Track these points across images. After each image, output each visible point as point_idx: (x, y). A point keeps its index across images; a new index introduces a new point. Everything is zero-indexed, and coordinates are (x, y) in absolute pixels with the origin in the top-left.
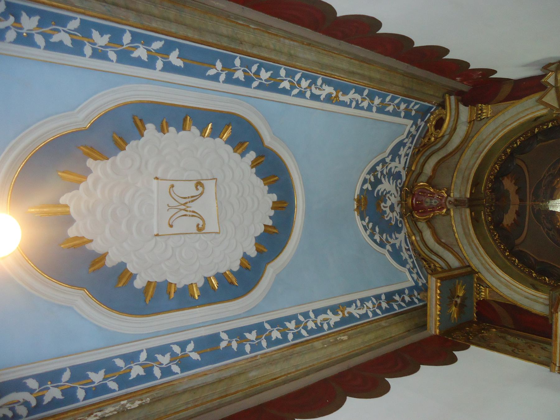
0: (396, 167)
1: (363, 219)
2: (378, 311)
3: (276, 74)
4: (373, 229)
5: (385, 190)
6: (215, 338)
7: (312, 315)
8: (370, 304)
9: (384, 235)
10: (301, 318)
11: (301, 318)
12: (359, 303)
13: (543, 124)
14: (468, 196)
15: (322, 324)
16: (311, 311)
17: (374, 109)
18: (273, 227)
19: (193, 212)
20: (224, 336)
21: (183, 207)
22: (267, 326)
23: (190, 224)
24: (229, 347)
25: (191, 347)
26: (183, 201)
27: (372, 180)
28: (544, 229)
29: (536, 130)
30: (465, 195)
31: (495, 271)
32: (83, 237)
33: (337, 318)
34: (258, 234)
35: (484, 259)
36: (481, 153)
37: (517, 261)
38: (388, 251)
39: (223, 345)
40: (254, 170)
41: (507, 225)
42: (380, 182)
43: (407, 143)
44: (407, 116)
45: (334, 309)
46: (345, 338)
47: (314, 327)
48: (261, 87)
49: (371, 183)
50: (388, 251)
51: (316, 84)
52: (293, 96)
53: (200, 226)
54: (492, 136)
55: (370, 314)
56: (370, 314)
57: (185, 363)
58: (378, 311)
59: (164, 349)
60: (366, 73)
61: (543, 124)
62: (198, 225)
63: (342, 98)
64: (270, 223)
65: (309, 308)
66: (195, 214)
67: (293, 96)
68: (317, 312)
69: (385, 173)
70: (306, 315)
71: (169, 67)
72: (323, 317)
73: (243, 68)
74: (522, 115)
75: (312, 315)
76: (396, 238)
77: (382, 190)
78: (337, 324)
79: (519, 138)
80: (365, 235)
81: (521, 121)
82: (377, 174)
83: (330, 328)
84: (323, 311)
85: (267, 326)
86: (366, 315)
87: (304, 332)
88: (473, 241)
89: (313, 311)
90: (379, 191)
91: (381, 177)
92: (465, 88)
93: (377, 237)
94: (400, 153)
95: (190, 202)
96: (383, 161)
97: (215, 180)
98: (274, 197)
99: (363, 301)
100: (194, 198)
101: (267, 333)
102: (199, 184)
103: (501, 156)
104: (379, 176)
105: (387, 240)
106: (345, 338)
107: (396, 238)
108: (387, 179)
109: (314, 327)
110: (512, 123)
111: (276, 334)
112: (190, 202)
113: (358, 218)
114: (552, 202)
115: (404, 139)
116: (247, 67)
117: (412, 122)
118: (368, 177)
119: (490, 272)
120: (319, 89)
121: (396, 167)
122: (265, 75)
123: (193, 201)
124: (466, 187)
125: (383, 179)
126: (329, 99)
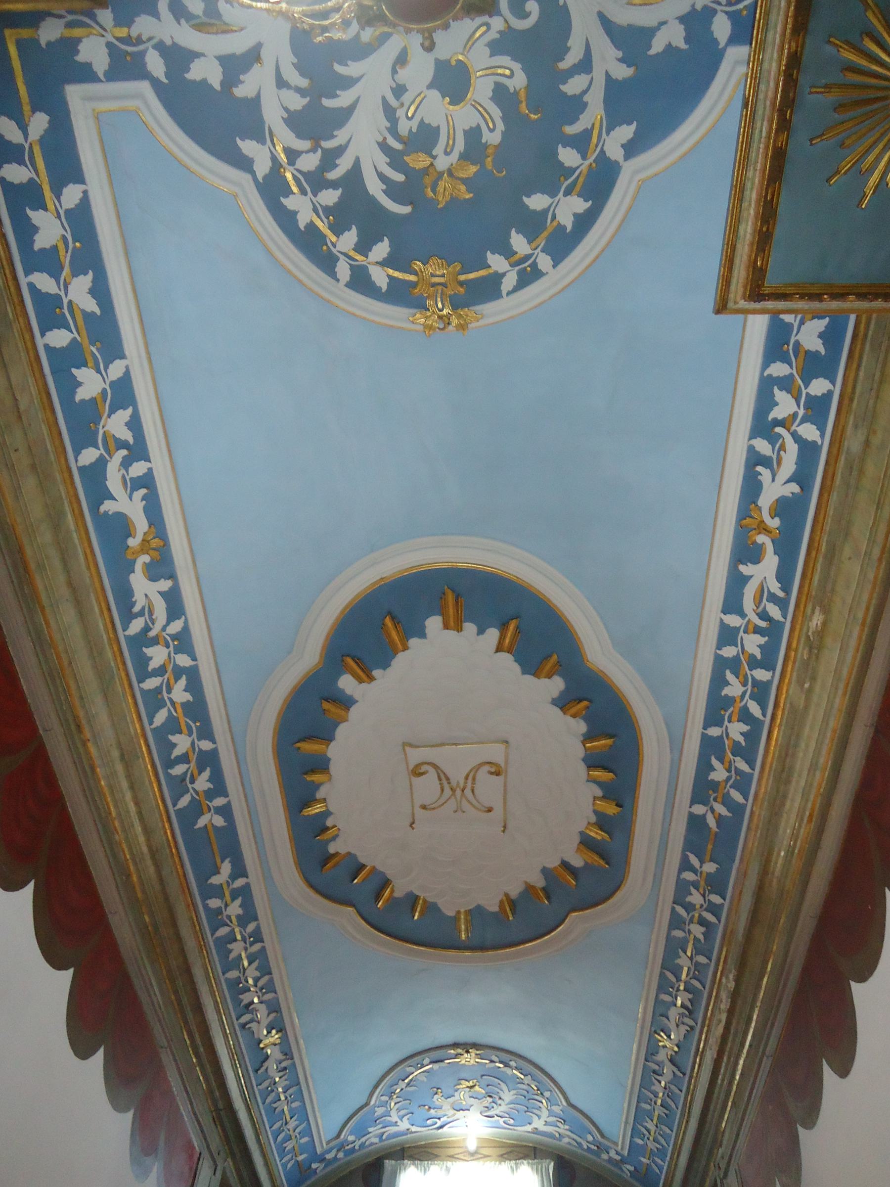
0: (281, 83)
1: (489, 289)
2: (819, 387)
3: (172, 725)
4: (533, 224)
5: (384, 146)
6: (696, 823)
7: (733, 620)
8: (785, 405)
9: (568, 156)
10: (729, 652)
11: (729, 652)
12: (763, 446)
15: (764, 615)
16: (722, 616)
17: (116, 370)
18: (503, 627)
19: (467, 778)
20: (699, 809)
21: (458, 792)
22: (714, 732)
23: (488, 788)
24: (719, 819)
25: (694, 861)
26: (448, 792)
27: (349, 239)
32: (501, 902)
33: (770, 562)
34: (517, 668)
38: (631, 149)
39: (711, 822)
40: (376, 673)
42: (353, 181)
43: (161, 47)
44: (65, 166)
45: (745, 552)
46: (817, 620)
47: (762, 640)
48: (206, 733)
49: (363, 247)
50: (631, 149)
51: (147, 629)
52: (194, 659)
53: (493, 770)
55: (809, 432)
56: (809, 432)
57: (716, 884)
58: (819, 387)
59: (682, 888)
60: (46, 536)
62: (492, 773)
63: (141, 525)
64: (493, 634)
65: (713, 616)
66: (471, 776)
67: (194, 659)
68: (732, 604)
69: (309, 162)
70: (727, 636)
71: (239, 871)
72: (749, 592)
73: (190, 786)
75: (733, 620)
76: (585, 65)
77: (382, 161)
78: (784, 576)
80: (556, 277)
82: (328, 211)
83: (783, 604)
84: (736, 583)
85: (714, 732)
86: (807, 450)
87: (761, 675)
89: (725, 611)
90: (392, 190)
91: (333, 185)
93: (568, 208)
94: (215, 78)
95: (449, 783)
96: (272, 189)
97: (407, 748)
98: (434, 623)
99: (763, 426)
100: (443, 776)
101: (726, 742)
102: (417, 772)
104: (329, 197)
105: (581, 143)
106: (817, 620)
107: (585, 65)
108: (340, 137)
109: (762, 640)
111: (736, 730)
112: (449, 783)
113: (491, 312)
115: (156, 83)
116: (184, 780)
117: (74, 93)
118: (343, 269)
120: (151, 613)
121: (281, 83)
122: (182, 743)
123: (448, 779)
125: (344, 164)
126: (162, 566)
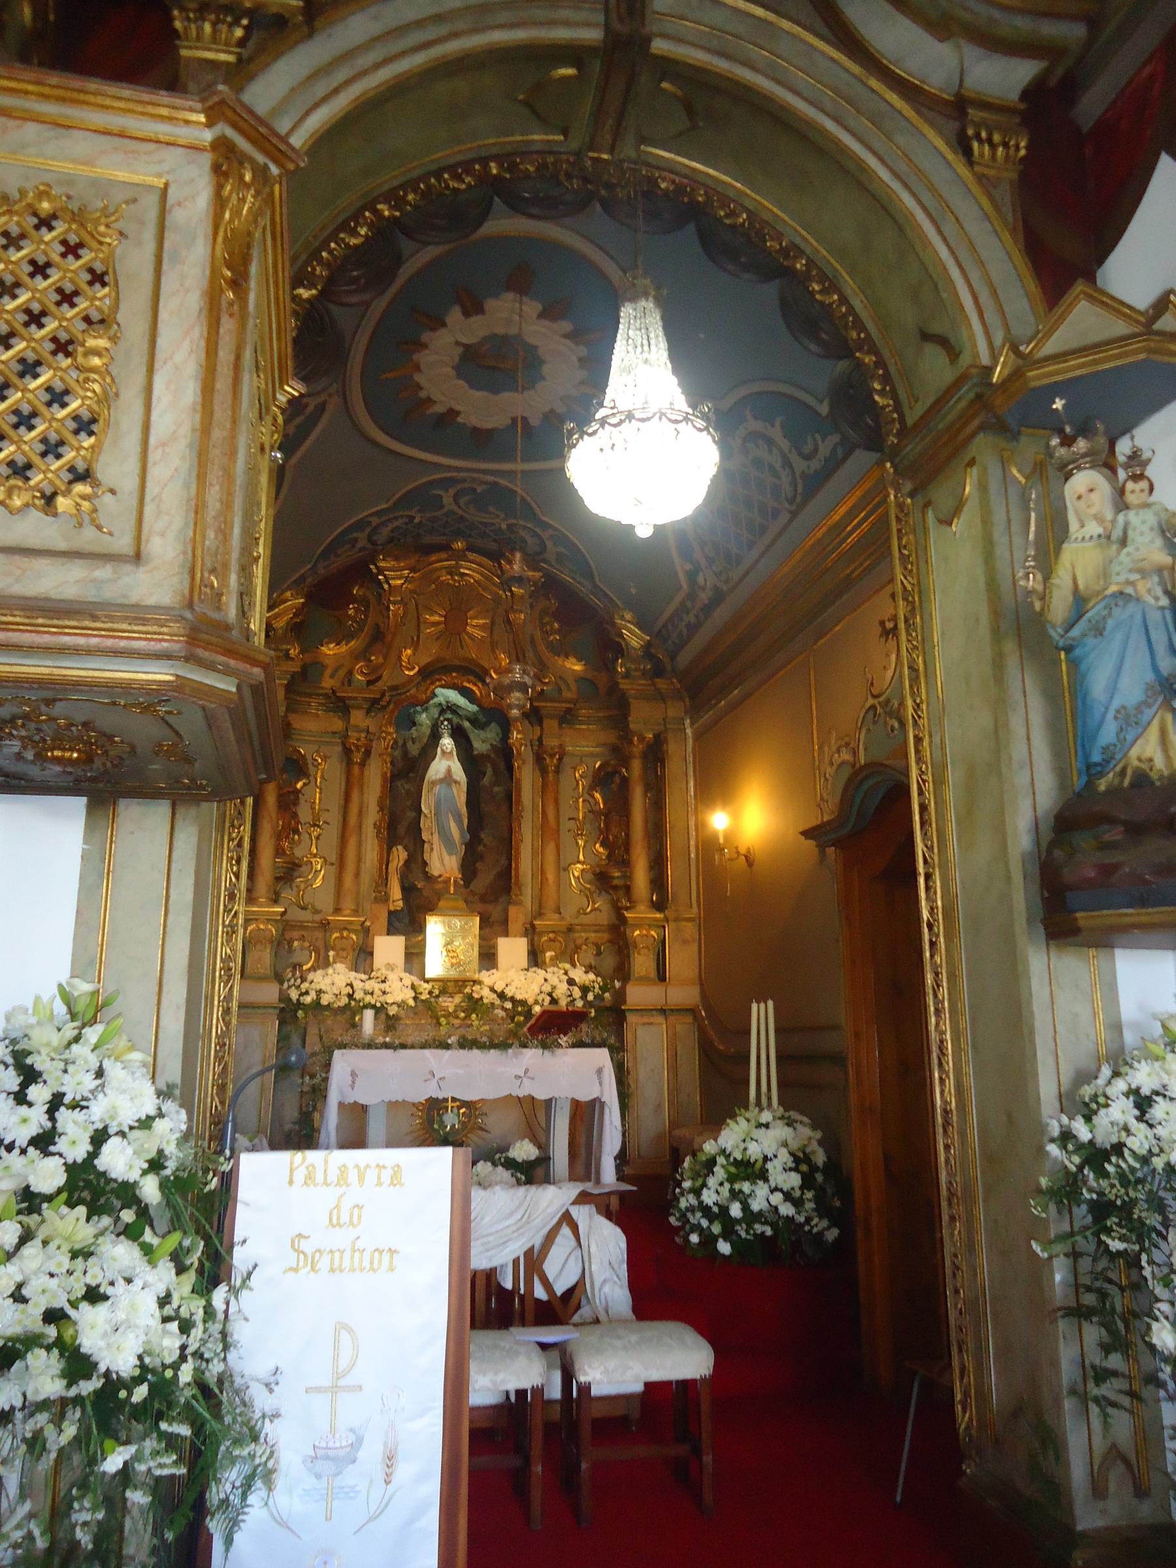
13: (886, 379)
14: (659, 46)
28: (378, 514)
29: (868, 359)
30: (664, 36)
31: (325, 99)
35: (378, 66)
36: (837, 120)
37: (354, 241)
41: (417, 368)
54: (902, 167)
61: (886, 379)
74: (975, 276)
79: (843, 300)
81: (955, 273)
88: (455, 35)
92: (1092, 105)
103: (779, 236)
110: (945, 240)
114: (655, 320)
119: (313, 77)
124: (694, 45)
